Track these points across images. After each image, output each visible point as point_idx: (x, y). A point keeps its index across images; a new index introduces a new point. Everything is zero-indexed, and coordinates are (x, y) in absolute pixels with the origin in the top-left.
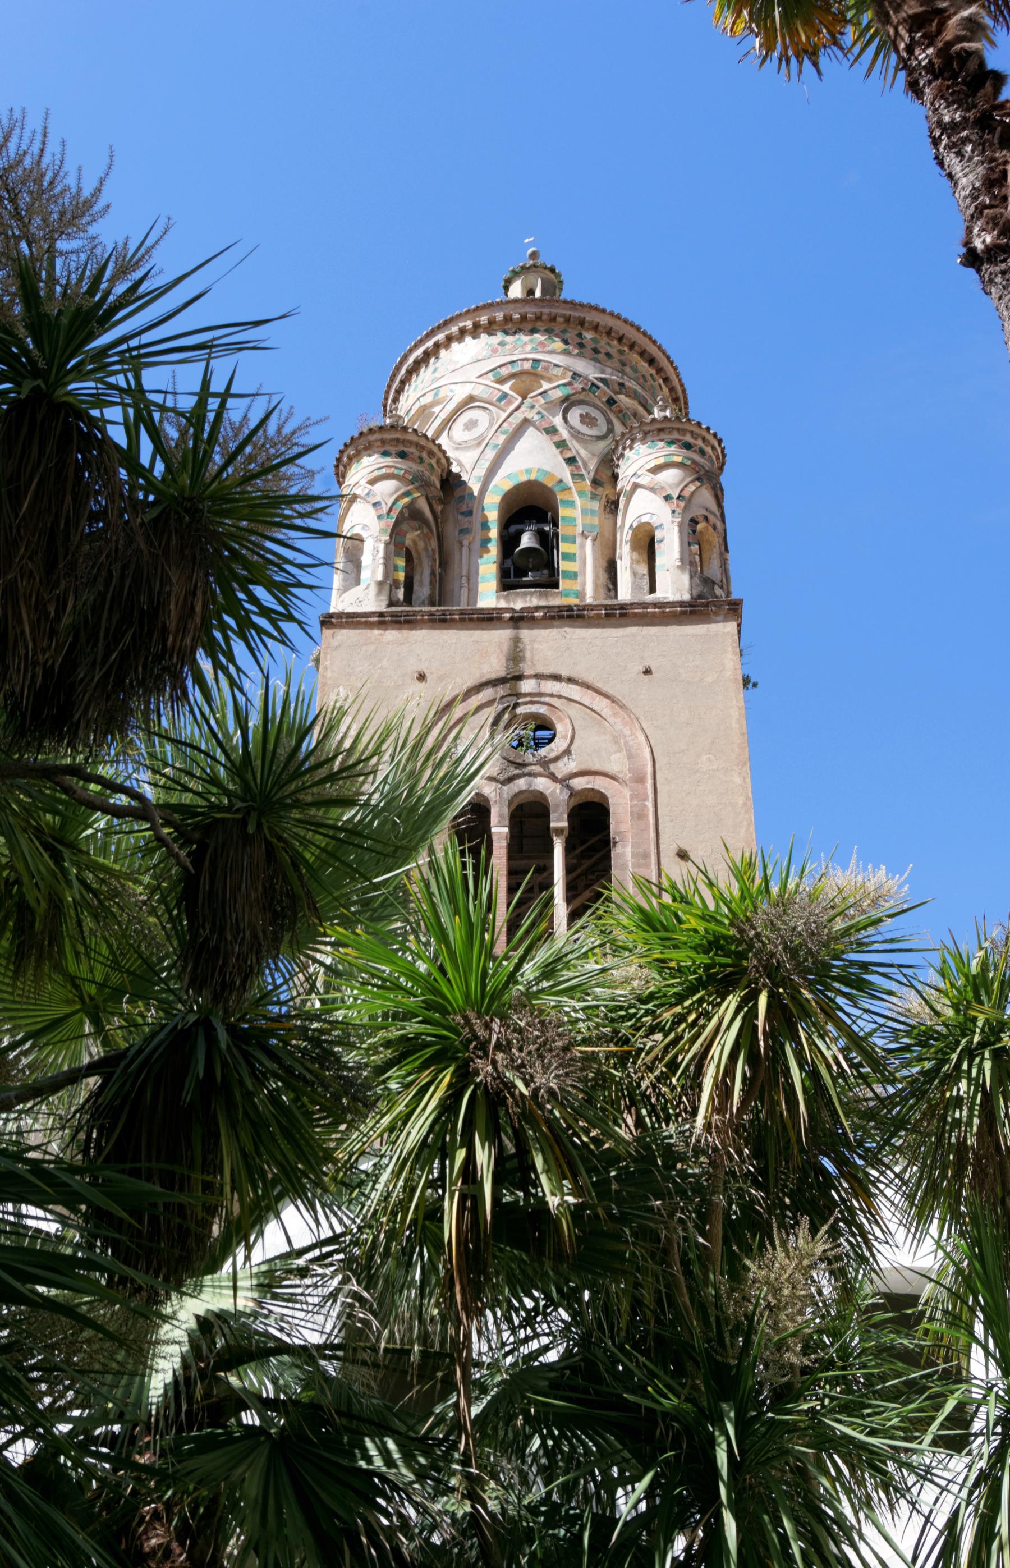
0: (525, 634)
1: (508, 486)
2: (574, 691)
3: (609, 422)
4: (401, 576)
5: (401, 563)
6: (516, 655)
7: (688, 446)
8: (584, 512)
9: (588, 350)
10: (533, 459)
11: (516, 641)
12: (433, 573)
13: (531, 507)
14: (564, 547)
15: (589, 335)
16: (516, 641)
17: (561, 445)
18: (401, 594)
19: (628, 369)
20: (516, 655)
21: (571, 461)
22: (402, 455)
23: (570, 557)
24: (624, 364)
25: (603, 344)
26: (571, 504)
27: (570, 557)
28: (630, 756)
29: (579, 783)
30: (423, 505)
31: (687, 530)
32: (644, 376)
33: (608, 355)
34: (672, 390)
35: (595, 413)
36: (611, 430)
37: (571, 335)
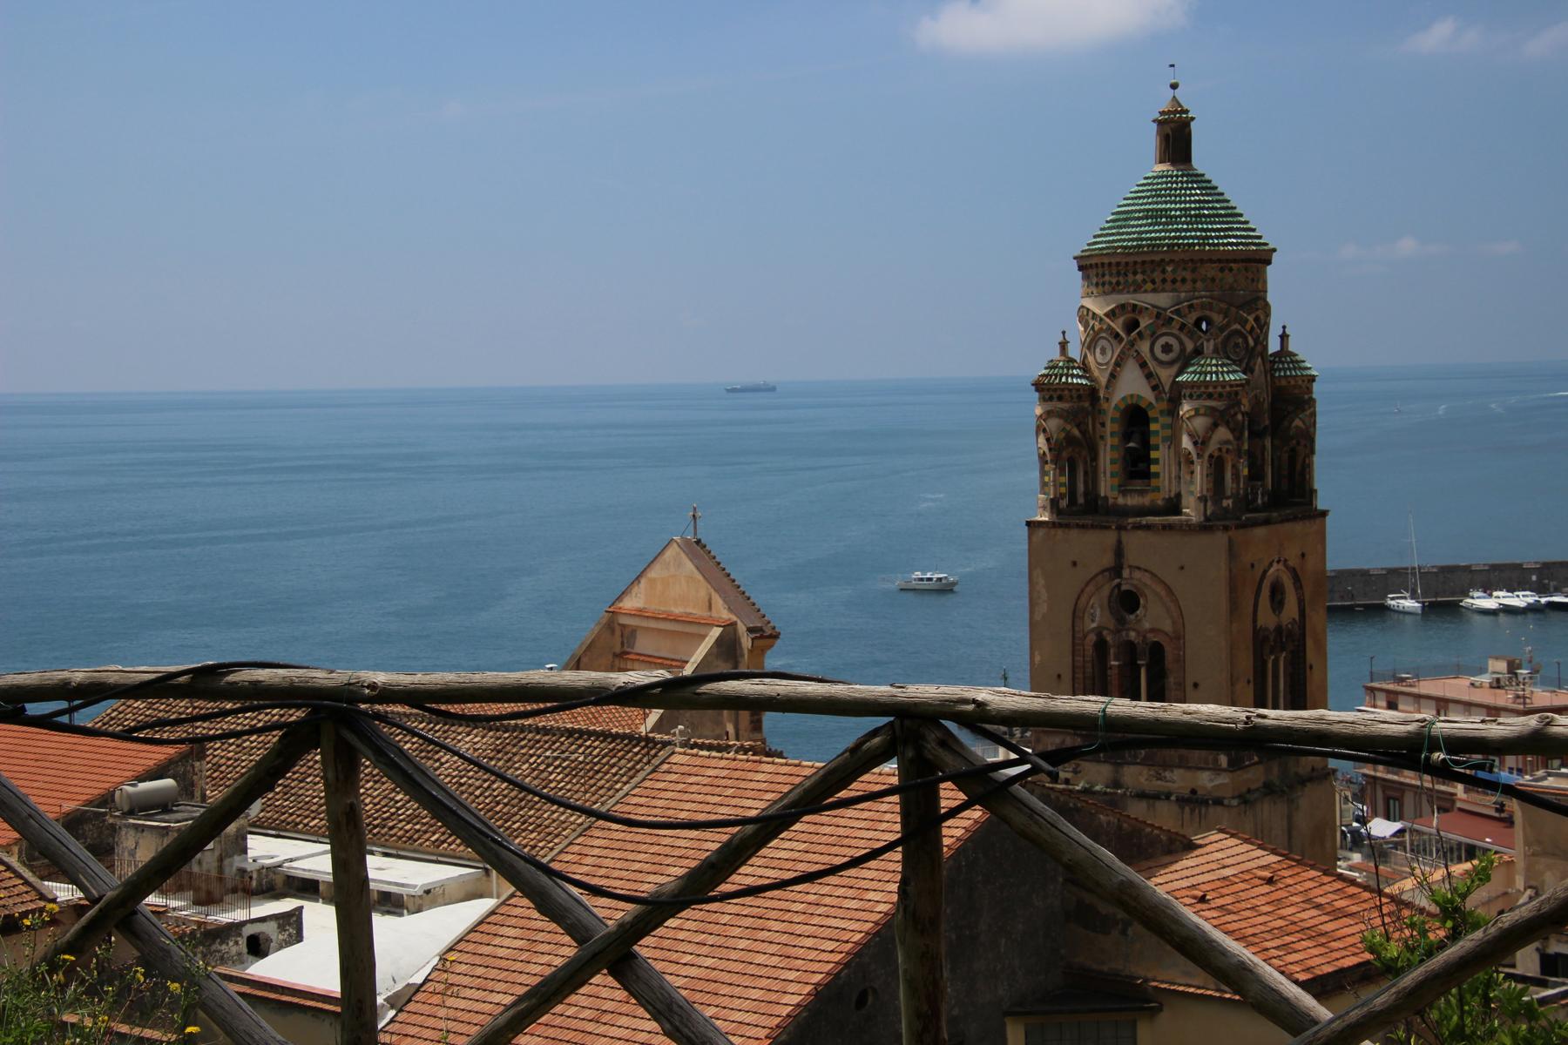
0: (1125, 536)
1: (1122, 406)
2: (1147, 579)
3: (1181, 343)
4: (1063, 490)
5: (1065, 479)
6: (1119, 552)
7: (1210, 396)
8: (1163, 427)
9: (1168, 285)
10: (1132, 385)
11: (1119, 542)
12: (1086, 473)
13: (1135, 417)
14: (1153, 455)
15: (1169, 269)
16: (1119, 542)
17: (1149, 376)
18: (1064, 503)
19: (1199, 284)
20: (1119, 552)
21: (1154, 388)
22: (1060, 398)
23: (1156, 461)
24: (1194, 281)
25: (1181, 274)
26: (1156, 420)
27: (1156, 461)
28: (1174, 623)
29: (1152, 638)
30: (1076, 432)
31: (1206, 464)
32: (1213, 280)
33: (1184, 280)
34: (1243, 261)
35: (1172, 341)
36: (1183, 349)
37: (1157, 276)
